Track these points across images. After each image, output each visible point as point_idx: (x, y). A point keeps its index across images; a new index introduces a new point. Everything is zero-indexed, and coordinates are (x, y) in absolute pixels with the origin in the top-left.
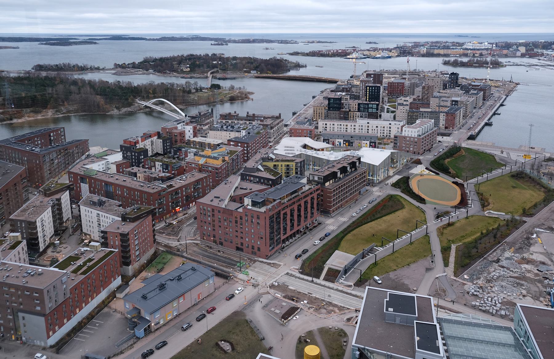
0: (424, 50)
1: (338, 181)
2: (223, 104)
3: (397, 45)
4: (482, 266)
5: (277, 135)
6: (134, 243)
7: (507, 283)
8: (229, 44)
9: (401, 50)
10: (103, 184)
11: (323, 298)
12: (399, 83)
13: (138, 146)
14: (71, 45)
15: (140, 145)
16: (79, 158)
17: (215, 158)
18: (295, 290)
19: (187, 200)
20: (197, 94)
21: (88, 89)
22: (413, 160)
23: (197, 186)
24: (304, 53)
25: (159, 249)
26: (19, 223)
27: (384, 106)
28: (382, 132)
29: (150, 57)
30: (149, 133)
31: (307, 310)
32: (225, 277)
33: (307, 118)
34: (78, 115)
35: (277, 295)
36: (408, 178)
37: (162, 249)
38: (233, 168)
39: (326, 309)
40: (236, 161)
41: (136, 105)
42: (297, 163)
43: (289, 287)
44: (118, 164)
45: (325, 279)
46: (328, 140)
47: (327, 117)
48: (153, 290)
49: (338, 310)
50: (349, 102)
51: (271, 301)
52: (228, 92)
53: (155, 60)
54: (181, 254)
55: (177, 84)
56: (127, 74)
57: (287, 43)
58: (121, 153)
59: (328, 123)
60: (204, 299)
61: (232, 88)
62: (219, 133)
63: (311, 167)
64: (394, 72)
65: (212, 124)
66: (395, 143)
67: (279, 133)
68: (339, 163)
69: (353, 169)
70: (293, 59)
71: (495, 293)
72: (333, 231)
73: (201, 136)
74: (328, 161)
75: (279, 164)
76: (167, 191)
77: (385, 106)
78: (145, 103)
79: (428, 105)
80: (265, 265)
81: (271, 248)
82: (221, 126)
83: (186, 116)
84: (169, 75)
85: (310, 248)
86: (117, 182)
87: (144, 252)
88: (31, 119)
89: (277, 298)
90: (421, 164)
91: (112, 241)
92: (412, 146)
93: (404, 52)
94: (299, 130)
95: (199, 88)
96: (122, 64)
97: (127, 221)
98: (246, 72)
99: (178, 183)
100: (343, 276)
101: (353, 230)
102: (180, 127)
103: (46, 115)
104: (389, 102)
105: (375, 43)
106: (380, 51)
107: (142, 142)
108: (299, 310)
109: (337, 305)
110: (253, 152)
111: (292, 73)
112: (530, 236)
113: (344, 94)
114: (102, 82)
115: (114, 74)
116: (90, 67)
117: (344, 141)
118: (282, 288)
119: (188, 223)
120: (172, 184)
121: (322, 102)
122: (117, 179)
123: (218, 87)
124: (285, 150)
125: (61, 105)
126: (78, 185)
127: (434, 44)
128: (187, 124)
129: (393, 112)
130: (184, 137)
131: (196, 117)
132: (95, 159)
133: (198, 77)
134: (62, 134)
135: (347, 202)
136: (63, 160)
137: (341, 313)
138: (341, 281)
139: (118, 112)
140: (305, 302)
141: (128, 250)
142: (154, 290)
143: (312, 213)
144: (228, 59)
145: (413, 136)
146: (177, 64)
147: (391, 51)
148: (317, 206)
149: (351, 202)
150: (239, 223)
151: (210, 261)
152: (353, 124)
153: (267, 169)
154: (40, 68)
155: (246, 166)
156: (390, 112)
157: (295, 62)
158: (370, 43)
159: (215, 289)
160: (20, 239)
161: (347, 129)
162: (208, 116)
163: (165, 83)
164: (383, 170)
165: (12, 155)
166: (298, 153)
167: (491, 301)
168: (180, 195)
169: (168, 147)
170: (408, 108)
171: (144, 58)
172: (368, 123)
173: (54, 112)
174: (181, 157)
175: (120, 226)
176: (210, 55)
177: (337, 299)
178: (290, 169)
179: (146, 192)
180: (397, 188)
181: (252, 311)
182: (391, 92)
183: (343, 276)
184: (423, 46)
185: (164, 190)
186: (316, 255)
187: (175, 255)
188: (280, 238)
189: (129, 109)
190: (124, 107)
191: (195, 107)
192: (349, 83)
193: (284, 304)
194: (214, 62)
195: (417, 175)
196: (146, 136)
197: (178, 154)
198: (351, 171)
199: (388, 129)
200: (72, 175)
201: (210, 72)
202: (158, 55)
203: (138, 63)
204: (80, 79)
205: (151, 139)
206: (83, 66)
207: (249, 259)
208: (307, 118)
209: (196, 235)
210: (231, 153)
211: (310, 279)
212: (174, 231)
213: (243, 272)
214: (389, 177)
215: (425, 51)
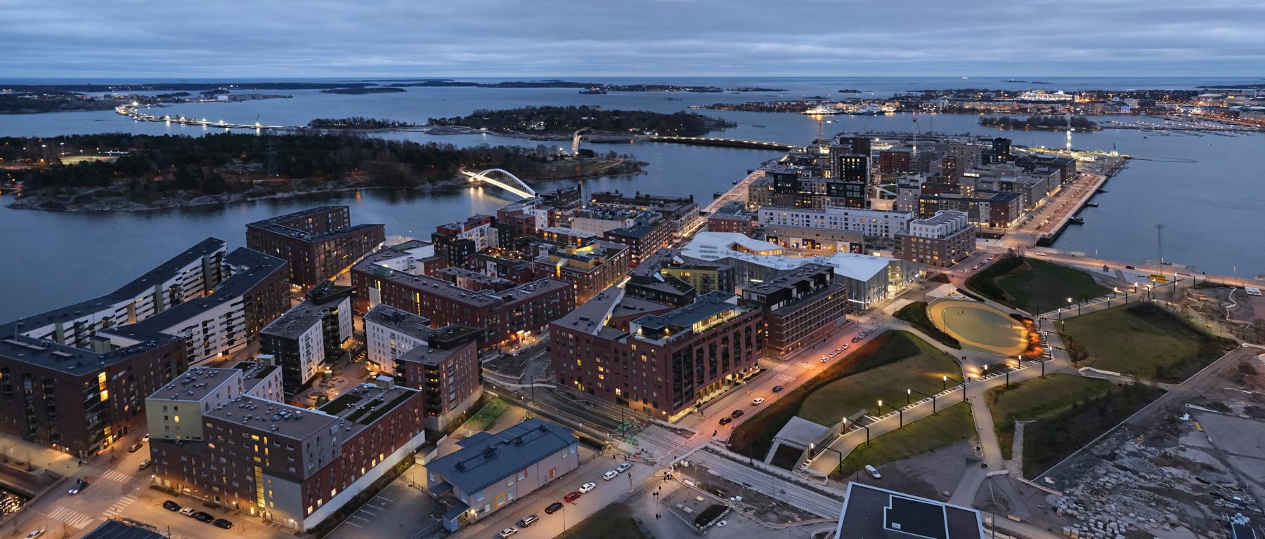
4: (1081, 464)
7: (1134, 499)
21: (388, 153)
63: (746, 279)
71: (1111, 515)
73: (562, 226)
74: (776, 271)
83: (536, 195)
112: (1176, 417)
114: (408, 144)
124: (701, 251)
164: (876, 290)
166: (722, 256)
167: (1104, 528)
190: (441, 180)
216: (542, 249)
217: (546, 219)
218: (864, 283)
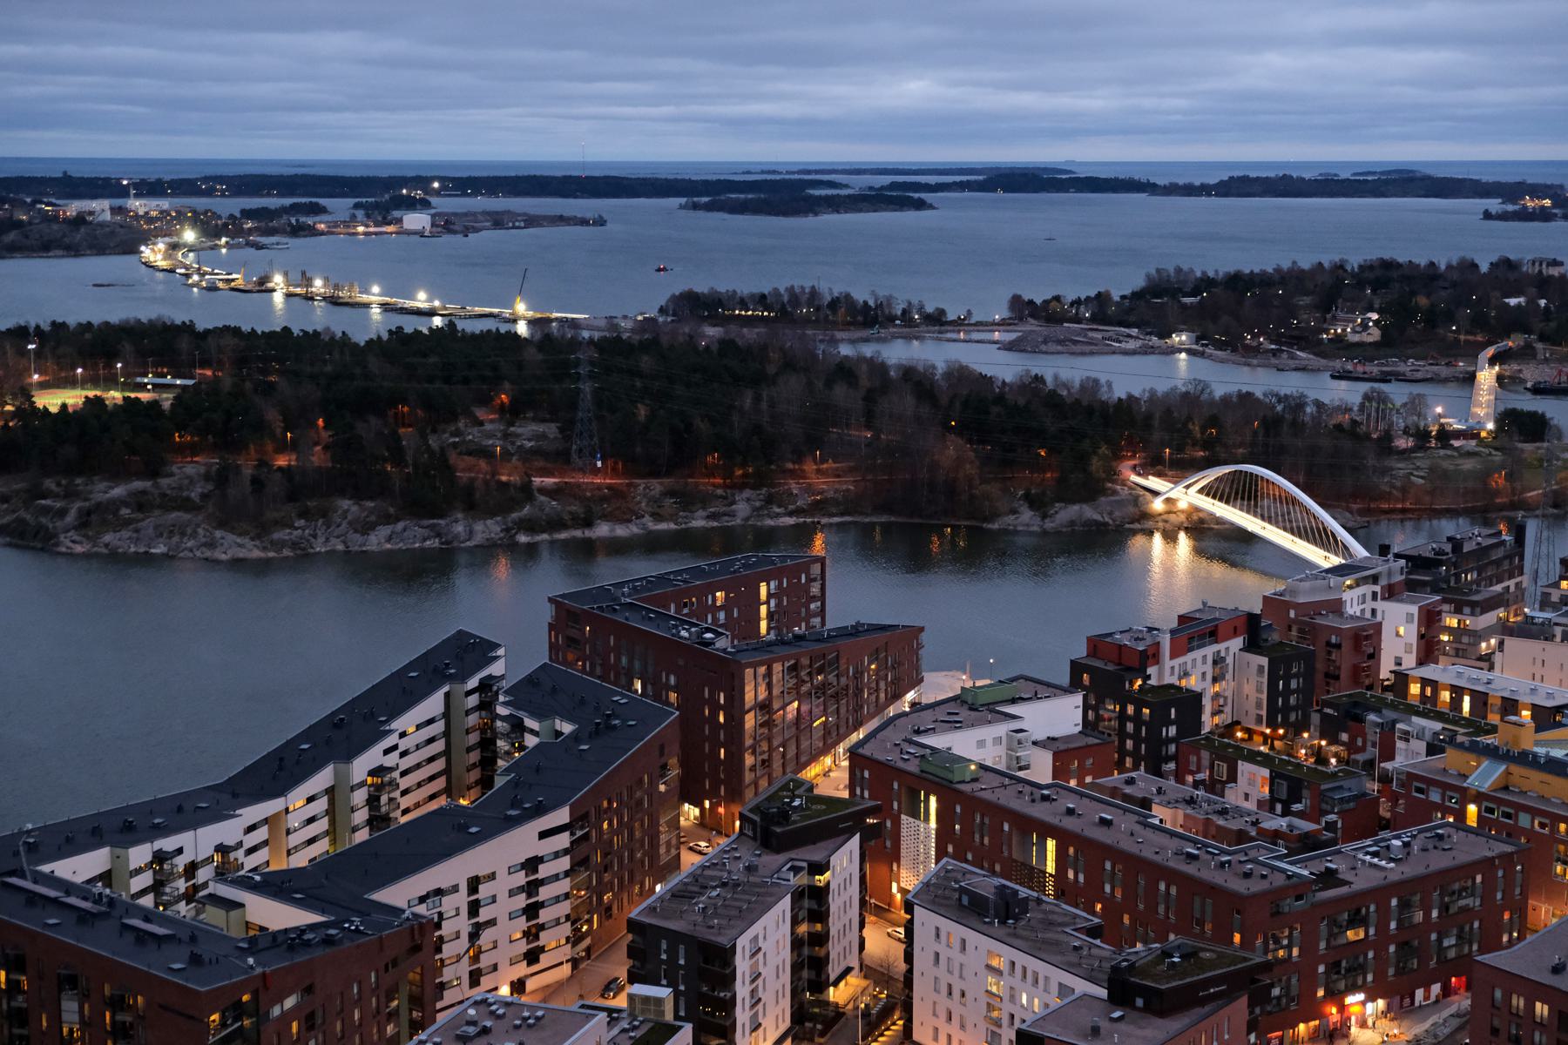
10: (1006, 827)
14: (816, 214)
15: (1164, 673)
16: (880, 709)
23: (1460, 897)
26: (664, 946)
29: (1179, 270)
30: (1205, 617)
34: (855, 523)
44: (1063, 747)
53: (1206, 283)
55: (1319, 405)
56: (1071, 347)
58: (1077, 699)
84: (1274, 361)
86: (1069, 823)
88: (663, 526)
95: (1434, 429)
96: (1045, 302)
97: (1134, 1008)
103: (725, 514)
107: (1172, 657)
115: (1009, 347)
116: (904, 312)
120: (1336, 870)
122: (1070, 812)
125: (791, 471)
126: (889, 824)
128: (1391, 593)
132: (965, 714)
133: (1419, 375)
134: (815, 589)
136: (817, 706)
139: (1038, 520)
154: (694, 305)
160: (669, 1017)
162: (1498, 563)
163: (1259, 394)
165: (618, 659)
168: (1372, 931)
169: (1293, 700)
171: (1148, 276)
173: (758, 504)
174: (1360, 757)
175: (1104, 1025)
176: (1484, 268)
179: (1213, 890)
185: (1298, 888)
189: (1089, 512)
191: (1409, 524)
194: (1513, 301)
197: (1344, 737)
200: (866, 774)
202: (1219, 262)
203: (1123, 297)
204: (862, 359)
205: (1215, 648)
206: (871, 303)
217: (1413, 639)
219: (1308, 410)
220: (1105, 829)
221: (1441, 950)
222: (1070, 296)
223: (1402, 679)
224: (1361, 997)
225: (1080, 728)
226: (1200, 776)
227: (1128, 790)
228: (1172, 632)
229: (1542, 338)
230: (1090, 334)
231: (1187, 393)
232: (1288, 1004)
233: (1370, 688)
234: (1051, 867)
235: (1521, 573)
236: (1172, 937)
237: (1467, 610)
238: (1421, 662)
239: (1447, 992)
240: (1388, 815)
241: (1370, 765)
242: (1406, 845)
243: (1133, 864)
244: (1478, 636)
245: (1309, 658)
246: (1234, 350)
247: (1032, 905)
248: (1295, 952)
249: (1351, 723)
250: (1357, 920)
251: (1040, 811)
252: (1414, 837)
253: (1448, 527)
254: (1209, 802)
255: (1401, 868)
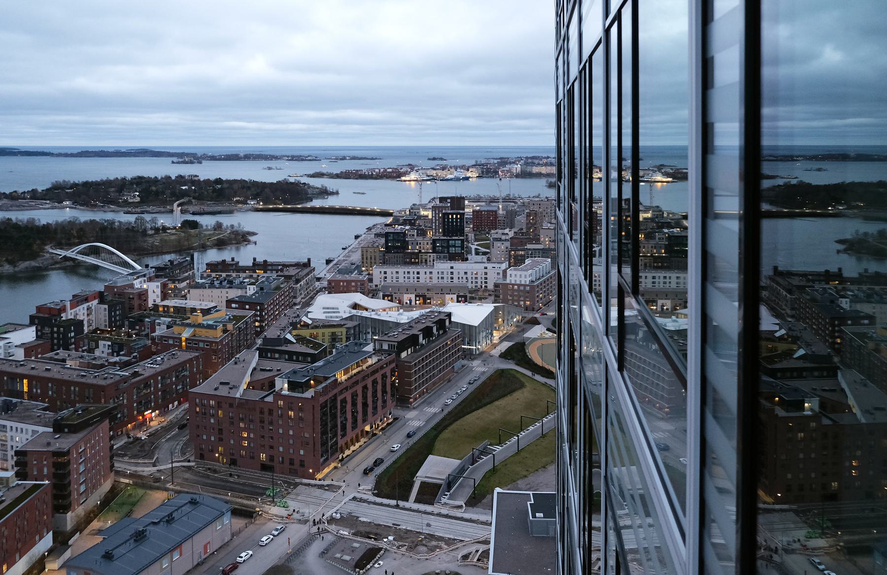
0: (517, 168)
1: (420, 350)
2: (206, 250)
3: (476, 162)
5: (306, 292)
6: (78, 468)
8: (203, 161)
9: (483, 168)
10: (5, 378)
11: (418, 529)
12: (490, 211)
13: (64, 316)
17: (209, 327)
18: (370, 523)
19: (164, 398)
20: (158, 238)
22: (526, 320)
23: (182, 372)
24: (332, 174)
25: (119, 482)
27: (470, 245)
28: (474, 281)
30: (83, 295)
31: (395, 551)
32: (248, 514)
33: (354, 264)
35: (341, 532)
36: (524, 343)
37: (127, 481)
38: (240, 344)
39: (426, 546)
40: (244, 332)
41: (48, 255)
42: (348, 329)
43: (360, 519)
44: (28, 346)
45: (417, 501)
46: (392, 296)
47: (385, 262)
48: (123, 544)
49: (446, 544)
50: (417, 239)
51: (333, 544)
52: (213, 232)
53: (75, 185)
54: (162, 486)
55: (119, 222)
56: (21, 208)
57: (303, 160)
58: (34, 328)
59: (389, 271)
60: (213, 553)
61: (219, 226)
62: (207, 292)
64: (478, 199)
65: (192, 280)
66: (496, 296)
67: (308, 290)
68: (418, 322)
69: (441, 332)
70: (317, 183)
72: (419, 429)
75: (320, 331)
76: (130, 382)
77: (471, 246)
78: (63, 253)
79: (538, 241)
80: (313, 489)
81: (322, 460)
82: (209, 282)
85: (386, 457)
86: (33, 373)
87: (95, 487)
89: (341, 538)
90: (539, 324)
91: (35, 469)
92: (522, 299)
93: (488, 171)
94: (343, 281)
98: (238, 202)
99: (148, 368)
100: (446, 493)
101: (451, 424)
102: (137, 284)
104: (476, 240)
105: (442, 159)
106: (453, 170)
107: (71, 310)
108: (382, 552)
109: (443, 538)
110: (270, 319)
111: (317, 203)
113: (408, 227)
117: (416, 296)
118: (348, 520)
119: (169, 436)
120: (138, 372)
121: (375, 240)
122: (33, 368)
123: (194, 225)
127: (530, 161)
128: (150, 280)
129: (484, 254)
130: (145, 300)
131: (167, 268)
135: (434, 384)
137: (451, 549)
138: (443, 500)
139: (13, 269)
140: (391, 538)
141: (66, 482)
142: (125, 542)
143: (384, 402)
144: (207, 182)
145: (523, 283)
146: (117, 191)
147: (468, 170)
148: (391, 389)
149: (441, 384)
150: (266, 422)
151: (217, 492)
152: (428, 271)
153: (300, 339)
155: (265, 336)
156: (481, 254)
157: (320, 187)
158: (434, 159)
159: (233, 535)
161: (418, 278)
162: (186, 266)
163: (98, 220)
168: (152, 389)
169: (118, 318)
170: (508, 244)
172: (452, 268)
174: (144, 333)
176: (173, 178)
177: (441, 528)
178: (337, 340)
180: (509, 359)
181: (302, 563)
182: (477, 226)
183: (446, 493)
184: (514, 163)
185: (125, 379)
186: (397, 465)
187: (151, 488)
188: (336, 443)
189: (33, 263)
191: (155, 257)
192: (412, 212)
193: (356, 545)
194: (184, 188)
195: (535, 340)
196: (78, 300)
197: (137, 327)
198: (439, 335)
199: (484, 276)
201: (177, 202)
202: (80, 178)
203: (43, 190)
205: (88, 304)
207: (285, 482)
208: (354, 264)
209: (185, 454)
210: (237, 319)
211: (393, 502)
212: (145, 451)
213: (278, 504)
214: (495, 346)
215: (519, 170)
216: (159, 324)
218: (476, 327)
219: (116, 224)
220: (48, 372)
221: (177, 390)
222: (21, 191)
223: (156, 307)
224: (150, 411)
225: (35, 338)
226: (84, 348)
227: (56, 357)
228: (70, 301)
229: (194, 198)
230: (30, 203)
231: (70, 221)
232: (124, 419)
233: (145, 310)
234: (26, 389)
235: (194, 269)
236: (77, 405)
237: (177, 282)
238: (162, 300)
239: (180, 404)
240: (155, 350)
241: (147, 335)
242: (162, 359)
243: (60, 383)
244: (181, 290)
245: (122, 303)
246: (87, 206)
247: (18, 404)
248: (125, 401)
249: (139, 323)
250: (147, 386)
251: (20, 370)
252: (165, 356)
253: (167, 258)
254: (89, 356)
255: (162, 366)
